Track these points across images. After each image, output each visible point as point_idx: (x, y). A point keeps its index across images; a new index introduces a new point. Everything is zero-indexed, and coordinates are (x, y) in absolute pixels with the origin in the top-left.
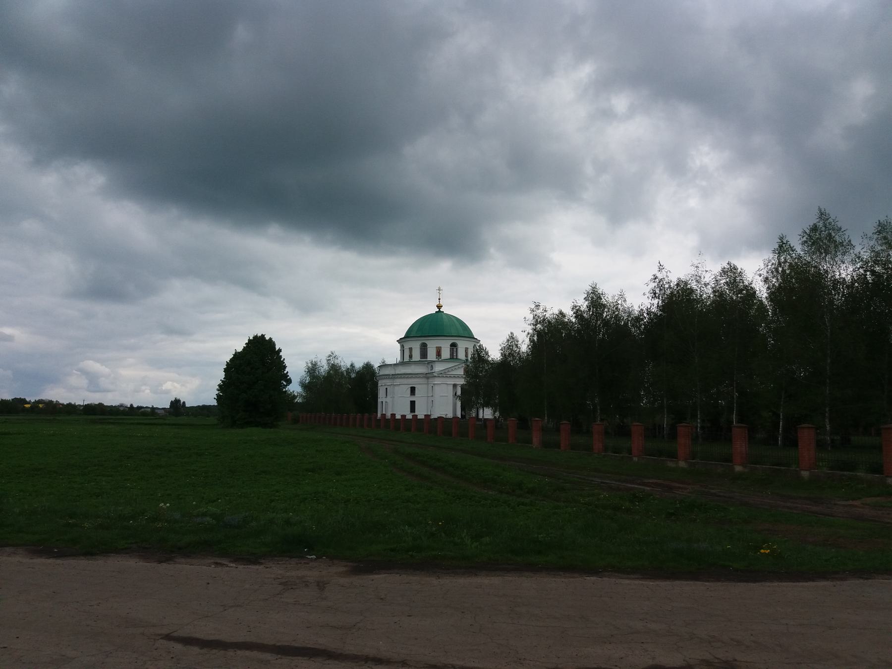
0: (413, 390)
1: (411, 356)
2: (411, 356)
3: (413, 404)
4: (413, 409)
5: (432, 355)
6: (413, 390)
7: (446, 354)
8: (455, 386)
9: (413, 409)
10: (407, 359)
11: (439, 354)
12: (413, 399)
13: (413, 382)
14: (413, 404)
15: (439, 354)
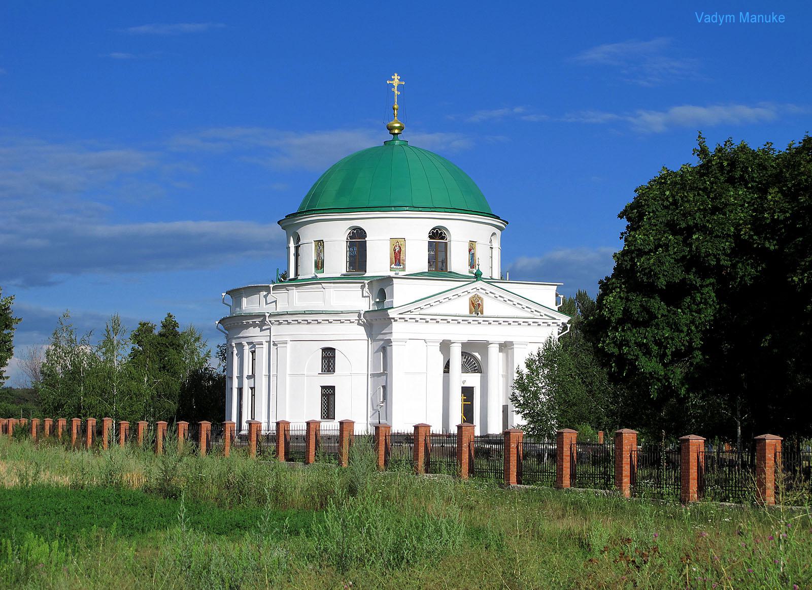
0: (329, 357)
1: (320, 265)
2: (320, 265)
3: (328, 394)
4: (328, 411)
5: (378, 263)
6: (329, 357)
7: (417, 257)
8: (445, 346)
9: (328, 411)
10: (308, 270)
11: (397, 258)
12: (328, 380)
13: (330, 334)
14: (328, 394)
15: (397, 258)
